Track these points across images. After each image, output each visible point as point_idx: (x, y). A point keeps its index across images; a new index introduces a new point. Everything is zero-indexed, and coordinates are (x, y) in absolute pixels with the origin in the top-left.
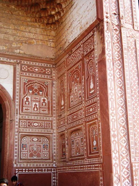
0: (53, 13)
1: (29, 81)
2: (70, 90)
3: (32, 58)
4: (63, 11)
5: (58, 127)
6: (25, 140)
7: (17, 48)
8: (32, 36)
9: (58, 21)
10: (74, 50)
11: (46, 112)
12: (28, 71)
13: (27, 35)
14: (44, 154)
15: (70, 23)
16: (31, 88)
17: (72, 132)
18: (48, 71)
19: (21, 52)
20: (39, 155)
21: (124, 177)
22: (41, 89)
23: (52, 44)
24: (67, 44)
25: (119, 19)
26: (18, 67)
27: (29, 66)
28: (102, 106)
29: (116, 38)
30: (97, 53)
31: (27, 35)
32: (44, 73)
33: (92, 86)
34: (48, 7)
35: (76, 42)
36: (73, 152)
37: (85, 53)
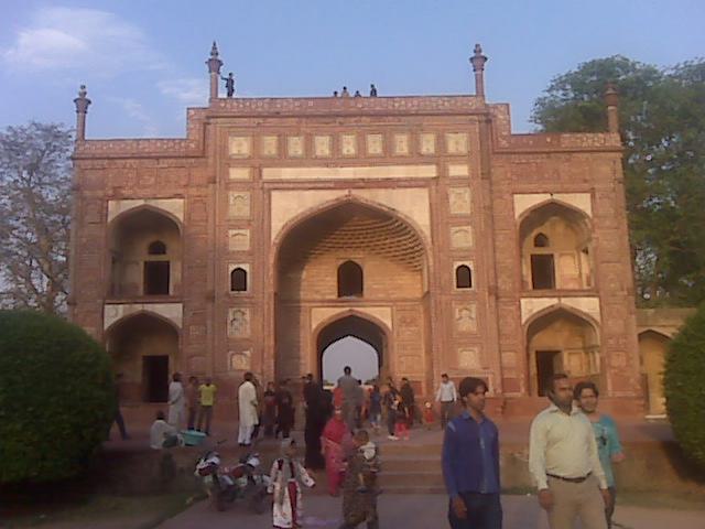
6: (402, 359)
22: (411, 322)
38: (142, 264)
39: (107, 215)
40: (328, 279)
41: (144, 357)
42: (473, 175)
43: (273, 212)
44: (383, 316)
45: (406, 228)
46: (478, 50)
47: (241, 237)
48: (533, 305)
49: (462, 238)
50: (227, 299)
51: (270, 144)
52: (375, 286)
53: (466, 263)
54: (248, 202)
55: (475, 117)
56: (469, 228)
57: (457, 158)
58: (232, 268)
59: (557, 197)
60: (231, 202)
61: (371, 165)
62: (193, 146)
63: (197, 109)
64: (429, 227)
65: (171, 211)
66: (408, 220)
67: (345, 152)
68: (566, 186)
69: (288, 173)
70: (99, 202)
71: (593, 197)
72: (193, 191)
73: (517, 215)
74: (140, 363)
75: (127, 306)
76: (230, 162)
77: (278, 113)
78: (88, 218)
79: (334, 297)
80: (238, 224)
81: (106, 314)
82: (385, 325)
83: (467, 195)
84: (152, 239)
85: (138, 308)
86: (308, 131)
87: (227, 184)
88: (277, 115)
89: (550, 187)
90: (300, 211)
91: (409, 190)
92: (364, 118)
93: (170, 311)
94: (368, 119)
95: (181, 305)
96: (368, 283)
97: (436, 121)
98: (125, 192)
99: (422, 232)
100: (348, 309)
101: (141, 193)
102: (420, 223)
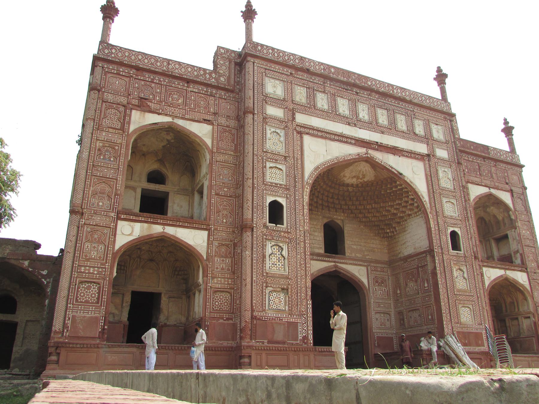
0: (388, 231)
1: (376, 277)
2: (406, 284)
3: (377, 262)
4: (396, 231)
5: (395, 308)
7: (368, 255)
8: (374, 246)
9: (391, 237)
10: (409, 260)
11: (387, 297)
12: (375, 270)
13: (371, 245)
14: (388, 324)
15: (403, 242)
16: (377, 282)
17: (410, 311)
18: (385, 270)
19: (370, 258)
20: (385, 325)
23: (386, 251)
24: (401, 255)
25: (442, 249)
26: (369, 268)
27: (375, 267)
28: (435, 297)
30: (430, 267)
31: (371, 245)
32: (383, 272)
33: (426, 285)
34: (385, 227)
35: (410, 256)
36: (412, 323)
37: (420, 265)
38: (139, 192)
39: (129, 123)
40: (316, 234)
41: (135, 294)
44: (359, 273)
45: (407, 192)
46: (439, 70)
47: (278, 172)
48: (492, 274)
50: (265, 230)
51: (300, 94)
52: (355, 247)
54: (282, 139)
56: (454, 201)
58: (270, 199)
59: (493, 191)
60: (268, 135)
61: (383, 133)
62: (222, 79)
63: (228, 50)
66: (412, 185)
67: (361, 116)
68: (497, 184)
70: (122, 109)
71: (512, 196)
72: (223, 121)
73: (472, 199)
74: (128, 298)
75: (146, 225)
76: (267, 99)
77: (308, 70)
78: (106, 122)
79: (322, 251)
80: (275, 157)
81: (118, 232)
82: (362, 283)
84: (155, 166)
85: (157, 229)
86: (332, 91)
87: (264, 118)
88: (307, 71)
89: (488, 183)
90: (329, 157)
92: (373, 94)
93: (195, 239)
95: (205, 233)
96: (348, 243)
97: (426, 114)
98: (152, 105)
101: (169, 110)
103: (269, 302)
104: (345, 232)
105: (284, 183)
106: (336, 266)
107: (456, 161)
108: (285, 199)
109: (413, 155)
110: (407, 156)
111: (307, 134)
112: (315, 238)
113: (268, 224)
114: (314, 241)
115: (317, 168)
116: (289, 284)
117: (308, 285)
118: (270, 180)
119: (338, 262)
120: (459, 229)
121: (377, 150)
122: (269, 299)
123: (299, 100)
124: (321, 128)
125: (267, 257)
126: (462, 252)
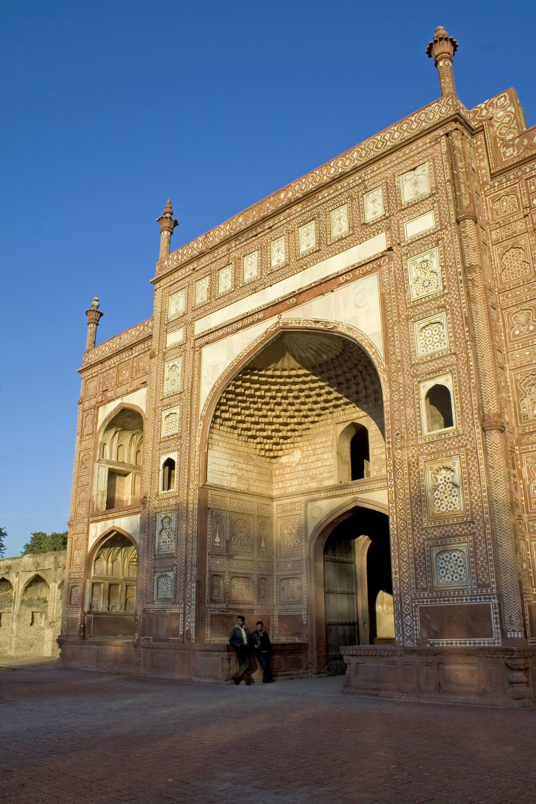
21: (405, 614)
29: (398, 464)
40: (325, 456)
42: (441, 226)
43: (204, 373)
49: (431, 340)
53: (441, 381)
55: (441, 132)
56: (442, 317)
57: (415, 207)
64: (381, 335)
65: (138, 404)
69: (217, 318)
83: (434, 258)
90: (229, 363)
91: (352, 286)
94: (298, 208)
99: (371, 346)
100: (351, 497)
102: (368, 332)
103: (158, 590)
104: (370, 435)
105: (176, 431)
106: (355, 500)
107: (453, 221)
108: (176, 453)
109: (357, 272)
110: (347, 281)
111: (207, 343)
112: (324, 464)
113: (161, 492)
114: (322, 469)
115: (212, 390)
116: (174, 565)
117: (193, 561)
118: (166, 435)
119: (358, 492)
120: (449, 376)
121: (296, 304)
122: (158, 586)
123: (201, 301)
124: (219, 325)
125: (157, 536)
126: (454, 428)
